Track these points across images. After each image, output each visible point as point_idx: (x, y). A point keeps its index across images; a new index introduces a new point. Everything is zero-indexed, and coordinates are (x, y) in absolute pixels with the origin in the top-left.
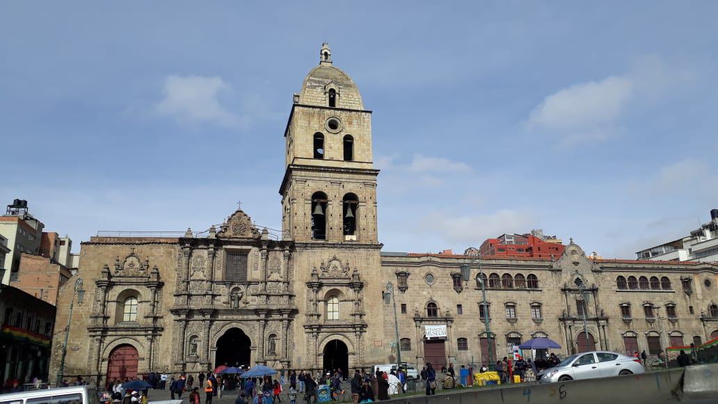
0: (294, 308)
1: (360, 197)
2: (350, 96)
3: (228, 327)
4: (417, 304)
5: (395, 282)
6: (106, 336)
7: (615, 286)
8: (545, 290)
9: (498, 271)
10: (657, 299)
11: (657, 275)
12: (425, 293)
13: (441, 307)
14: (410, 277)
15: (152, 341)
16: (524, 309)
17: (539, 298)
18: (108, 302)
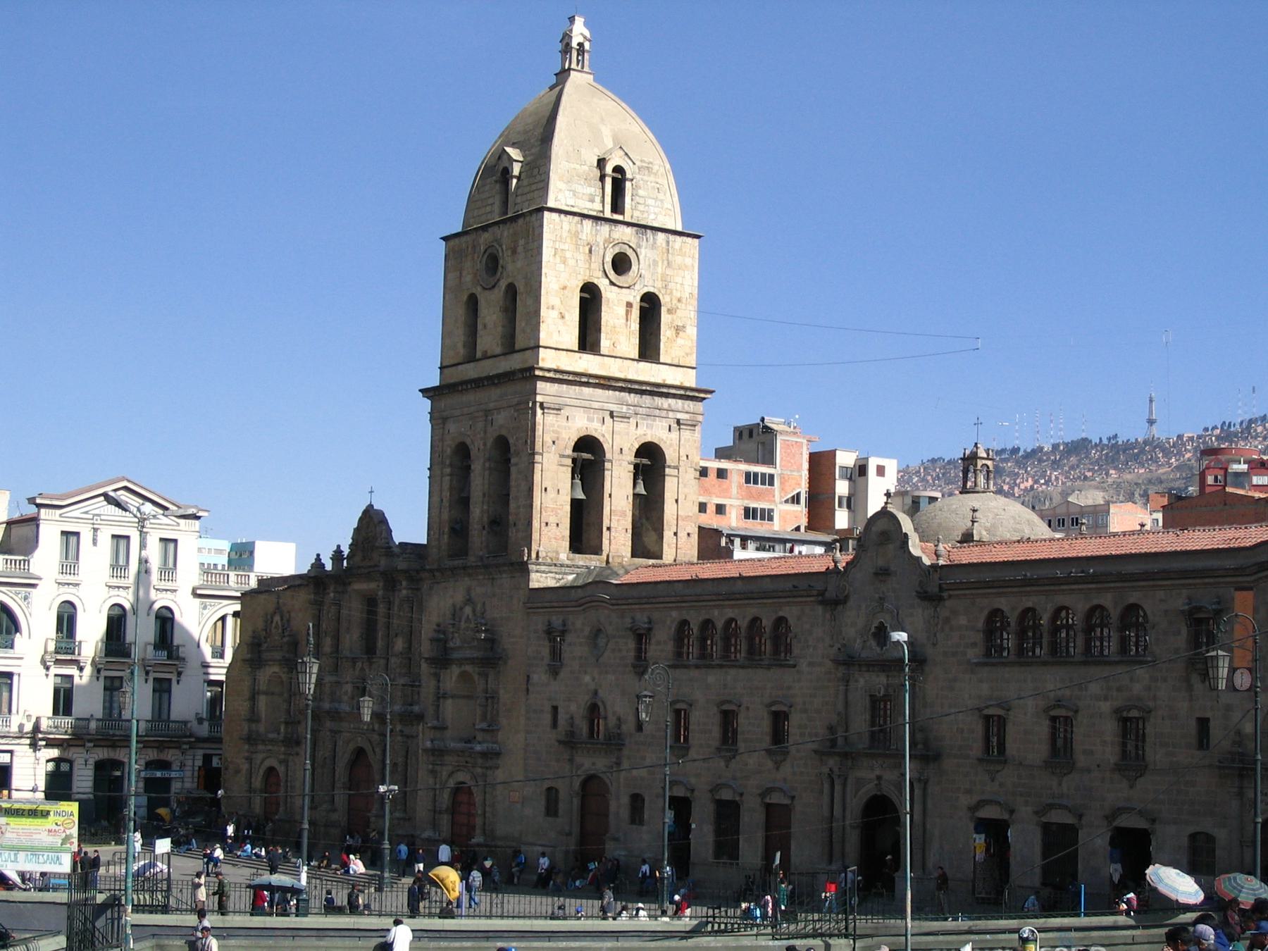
0: (416, 709)
1: (511, 441)
2: (536, 171)
3: (352, 746)
4: (573, 707)
5: (546, 652)
6: (256, 752)
7: (974, 645)
8: (803, 666)
9: (716, 612)
10: (1094, 688)
11: (1107, 600)
12: (587, 679)
13: (610, 716)
14: (569, 638)
15: (285, 762)
16: (753, 726)
17: (789, 688)
18: (258, 693)
